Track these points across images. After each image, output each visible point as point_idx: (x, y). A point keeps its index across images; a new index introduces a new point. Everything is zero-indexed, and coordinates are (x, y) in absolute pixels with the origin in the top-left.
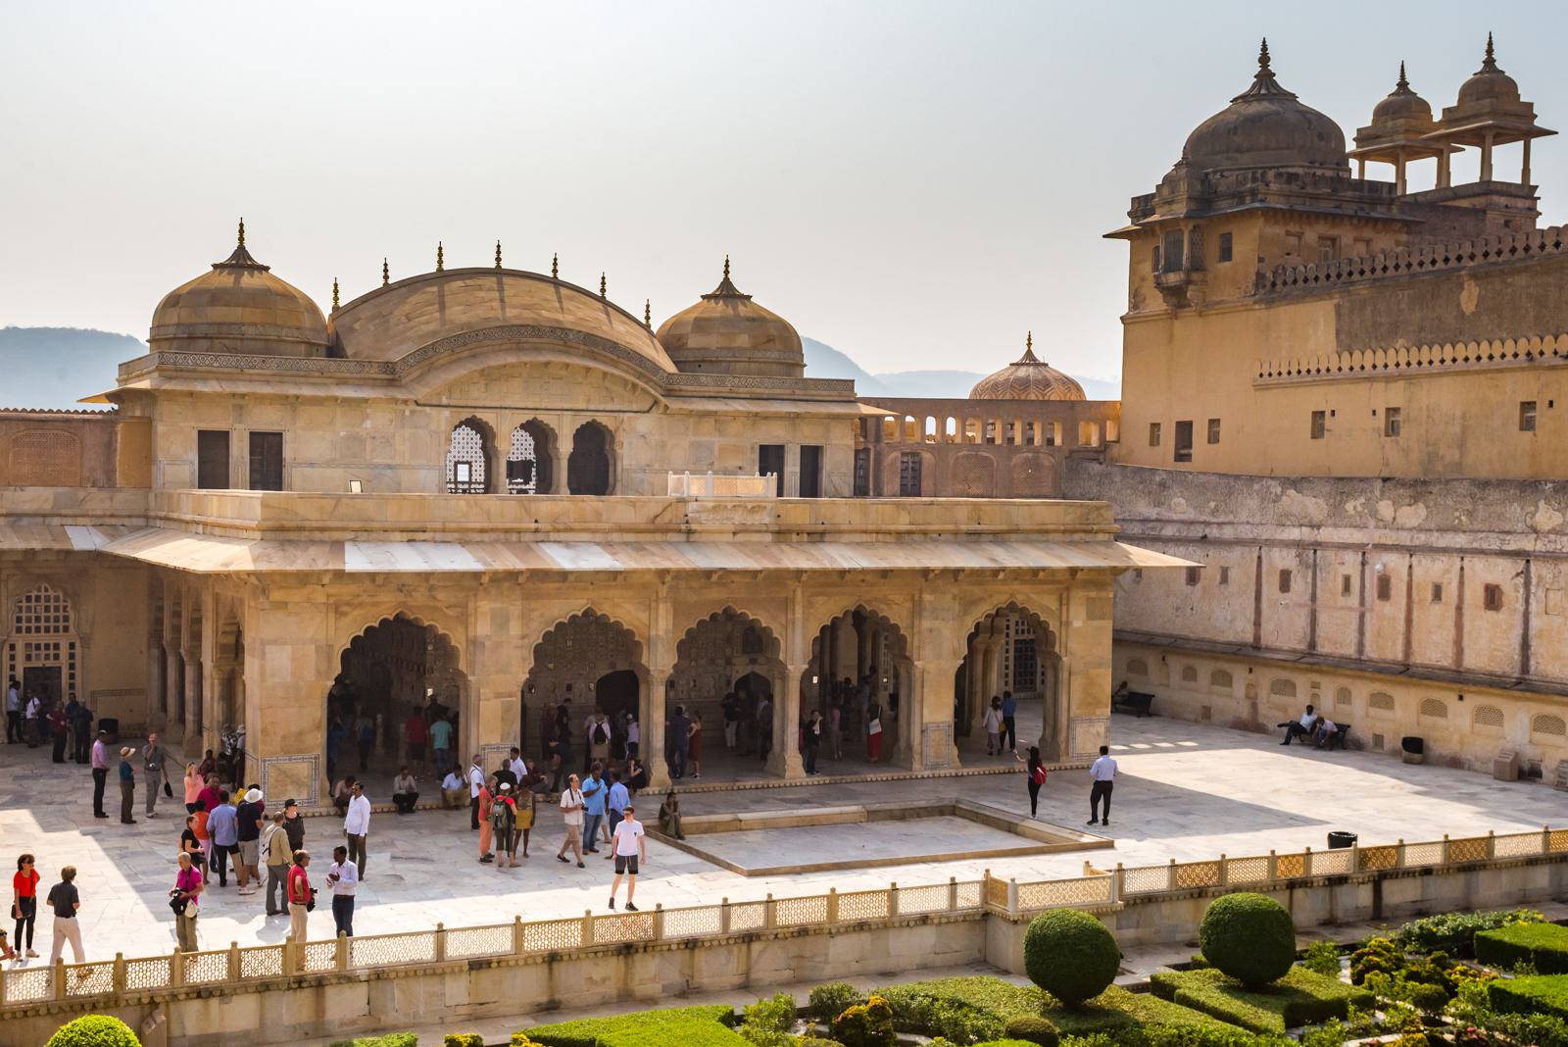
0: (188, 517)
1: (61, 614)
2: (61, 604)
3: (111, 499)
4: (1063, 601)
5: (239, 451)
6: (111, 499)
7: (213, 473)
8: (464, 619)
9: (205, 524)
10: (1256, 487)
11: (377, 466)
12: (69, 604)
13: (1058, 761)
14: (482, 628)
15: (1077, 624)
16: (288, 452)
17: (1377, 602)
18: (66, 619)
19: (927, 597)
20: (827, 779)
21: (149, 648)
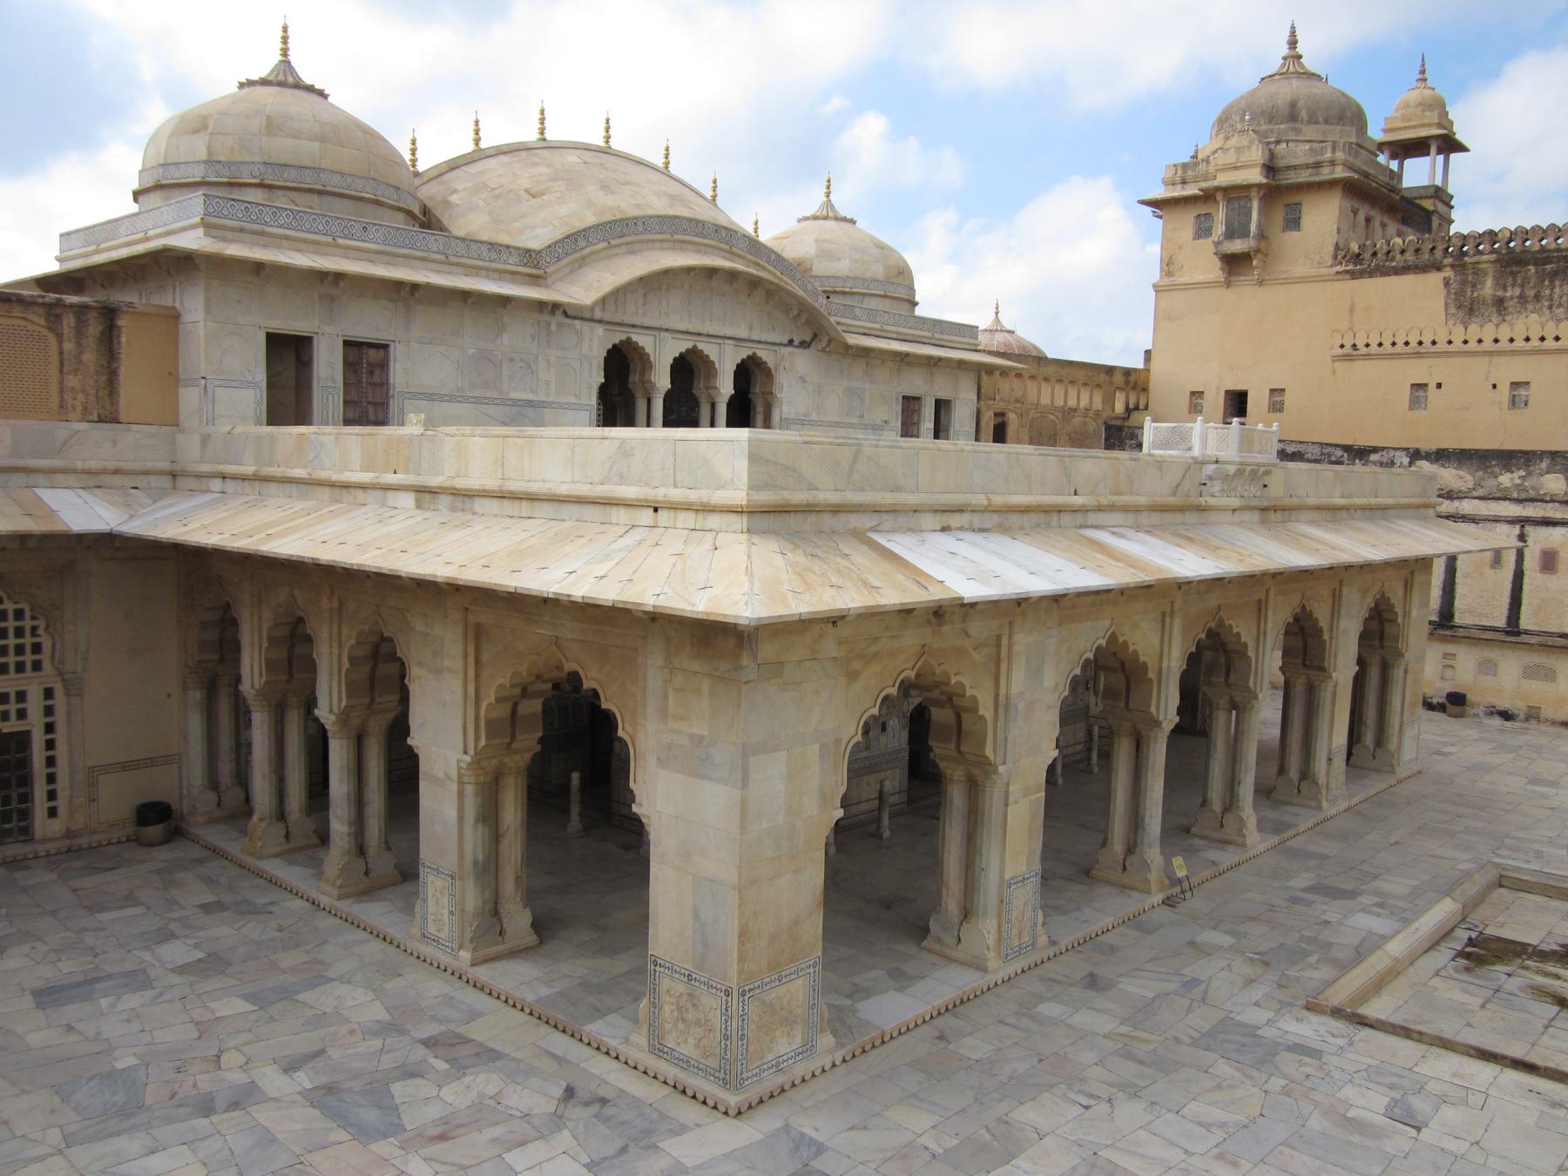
0: (366, 477)
1: (28, 640)
2: (28, 623)
3: (115, 443)
4: (1408, 586)
5: (328, 365)
6: (115, 443)
7: (288, 401)
8: (996, 666)
9: (420, 490)
10: (1373, 457)
11: (515, 403)
12: (41, 623)
13: (1393, 772)
14: (1017, 681)
15: (1414, 613)
16: (399, 374)
17: (1539, 575)
18: (37, 648)
19: (1345, 590)
20: (1275, 840)
21: (185, 688)
